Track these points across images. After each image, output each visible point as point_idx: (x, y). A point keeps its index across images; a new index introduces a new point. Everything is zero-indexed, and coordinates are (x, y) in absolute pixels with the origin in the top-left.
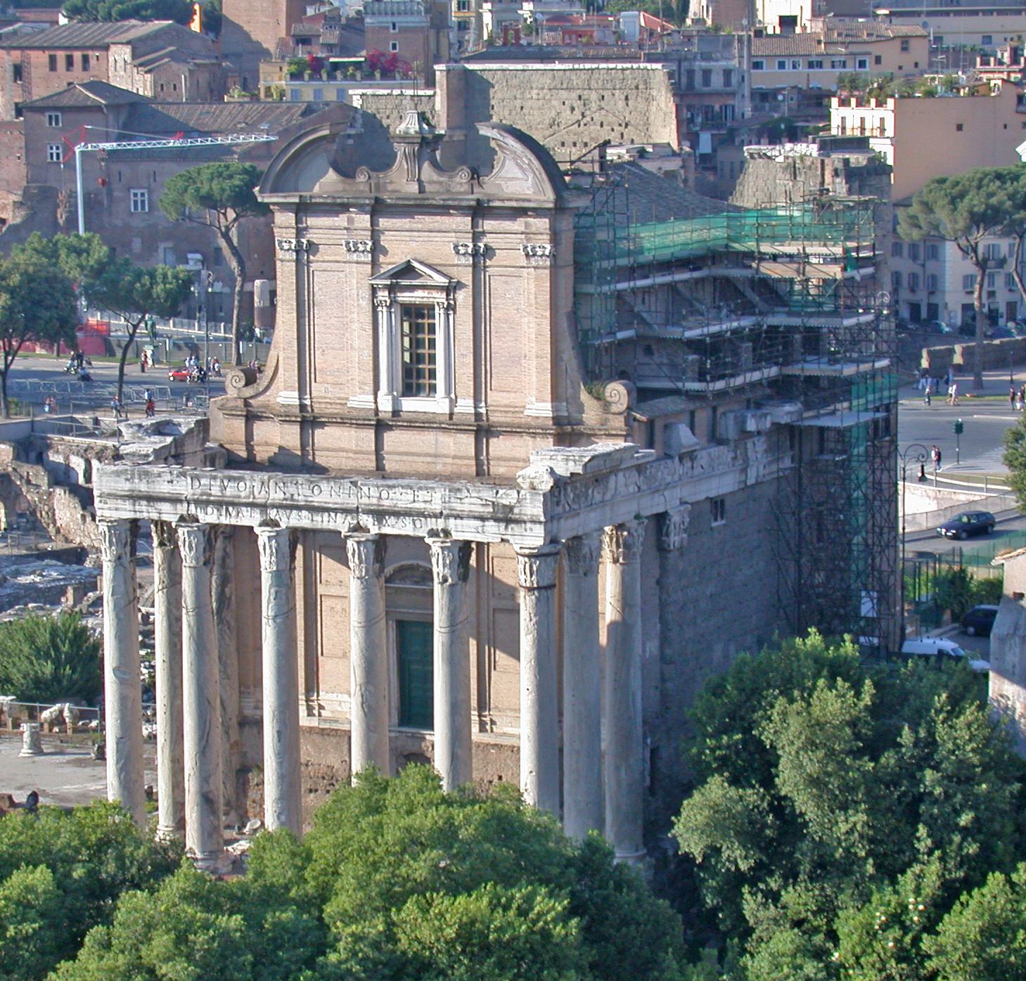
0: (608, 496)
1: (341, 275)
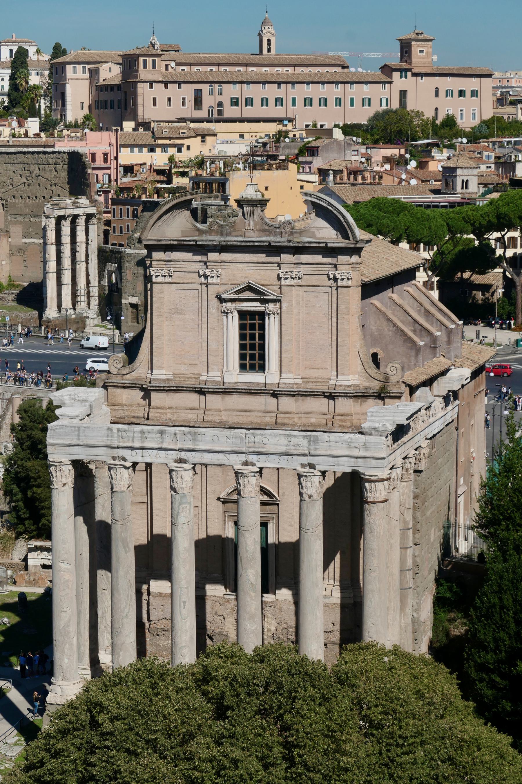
1: (196, 292)
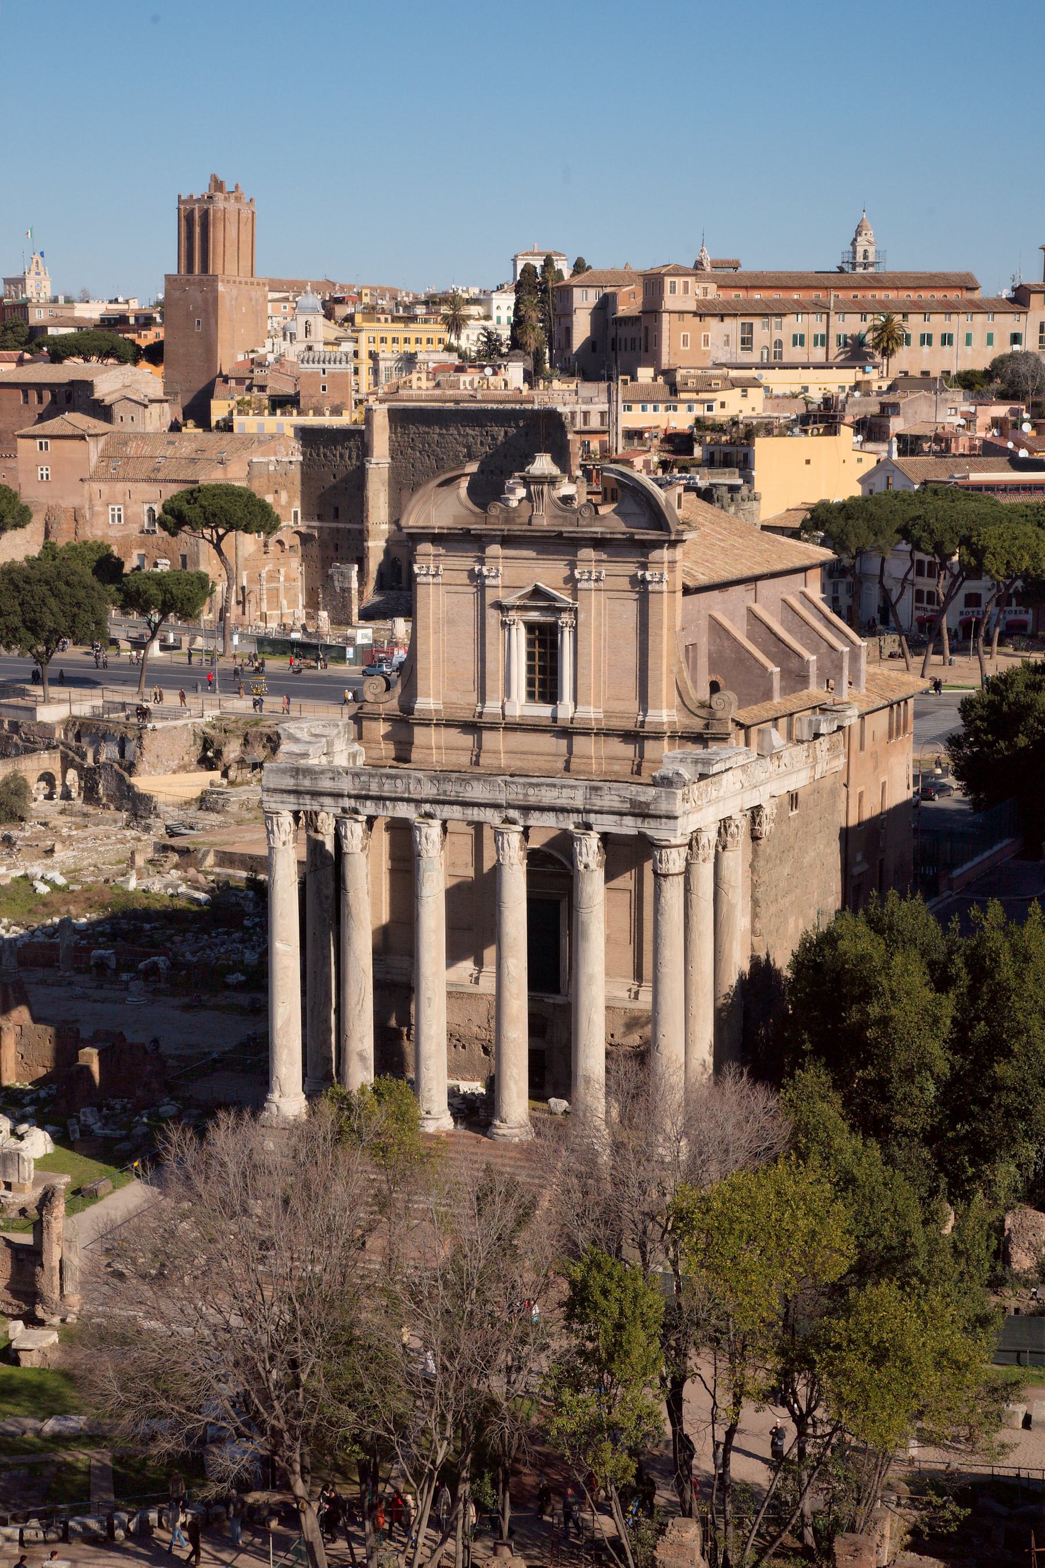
0: (721, 794)
